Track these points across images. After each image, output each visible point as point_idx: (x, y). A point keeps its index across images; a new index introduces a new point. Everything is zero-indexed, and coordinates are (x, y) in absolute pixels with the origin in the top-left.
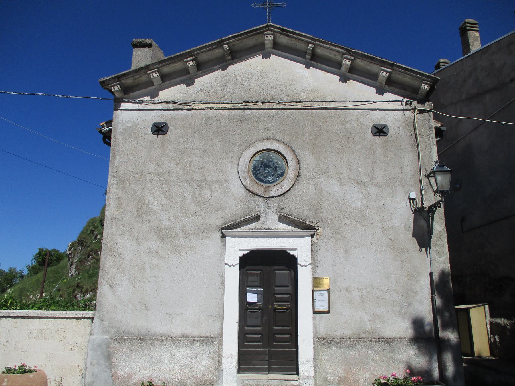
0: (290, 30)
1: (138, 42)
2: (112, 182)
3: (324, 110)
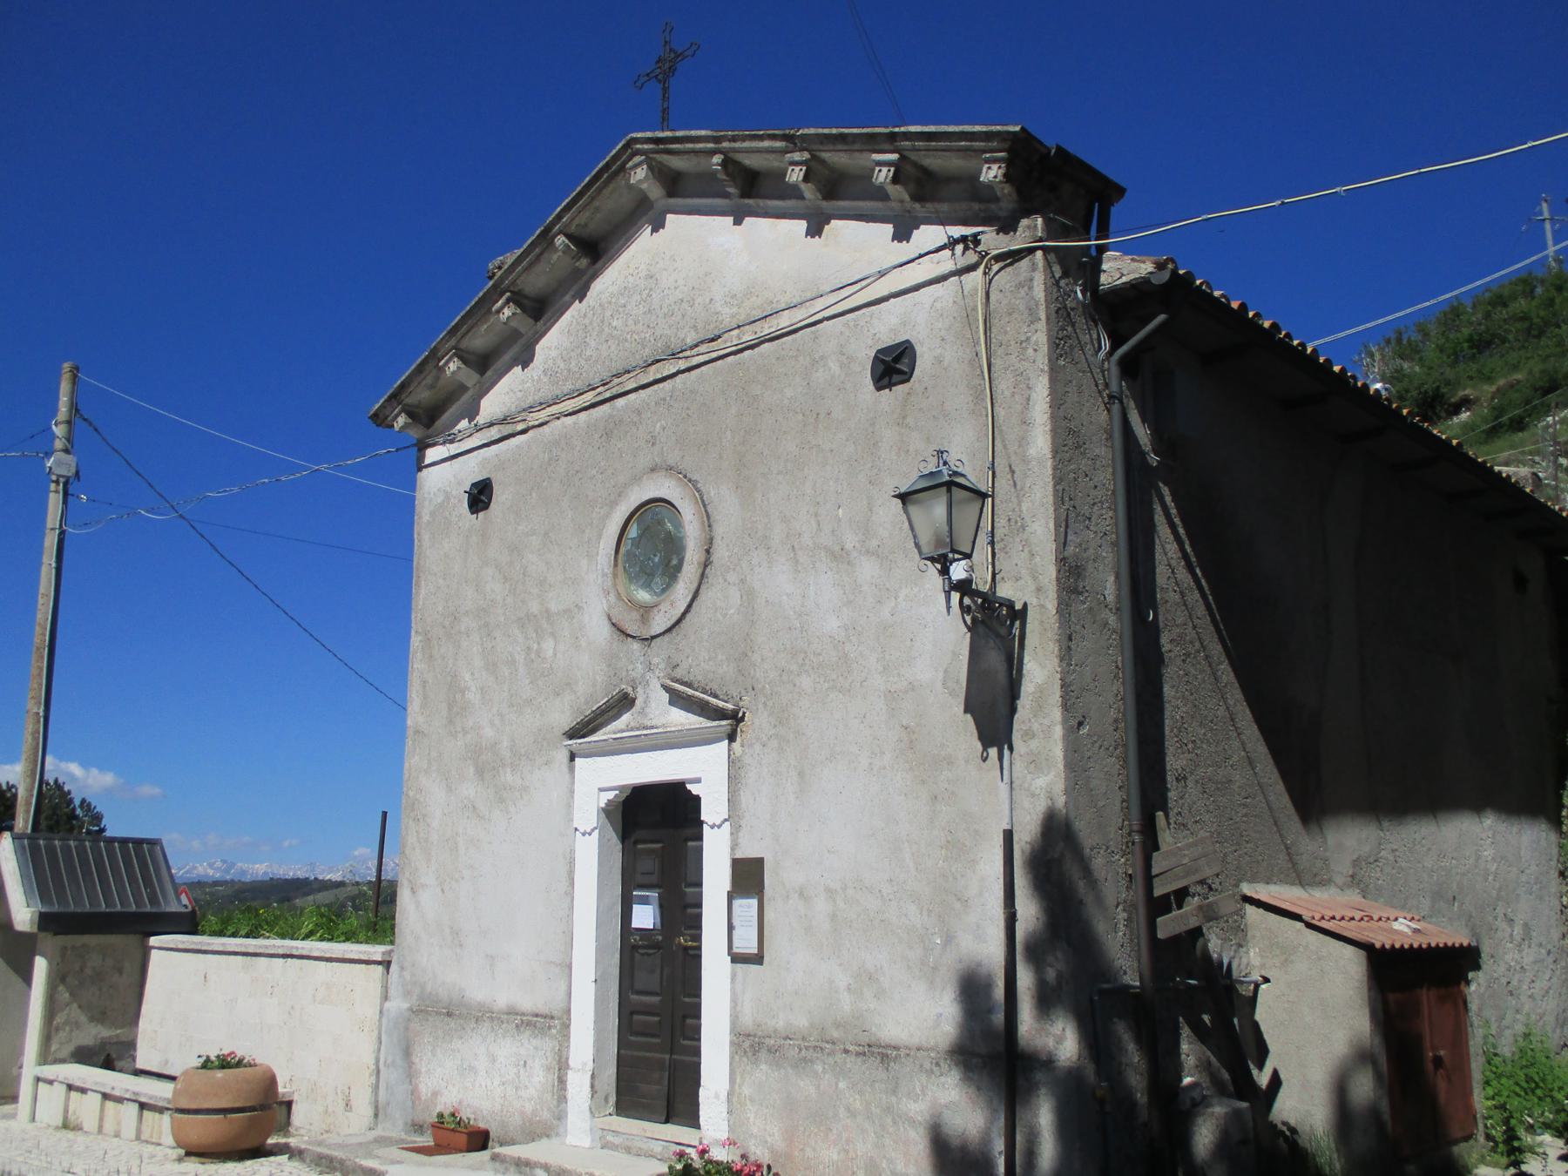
3: (766, 345)
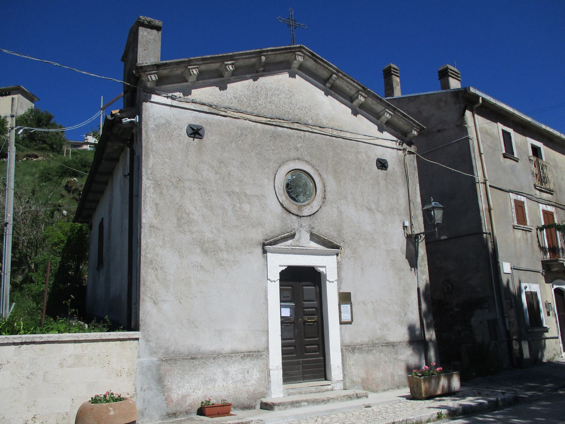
0: (320, 56)
1: (147, 21)
2: (148, 185)
3: (341, 139)
